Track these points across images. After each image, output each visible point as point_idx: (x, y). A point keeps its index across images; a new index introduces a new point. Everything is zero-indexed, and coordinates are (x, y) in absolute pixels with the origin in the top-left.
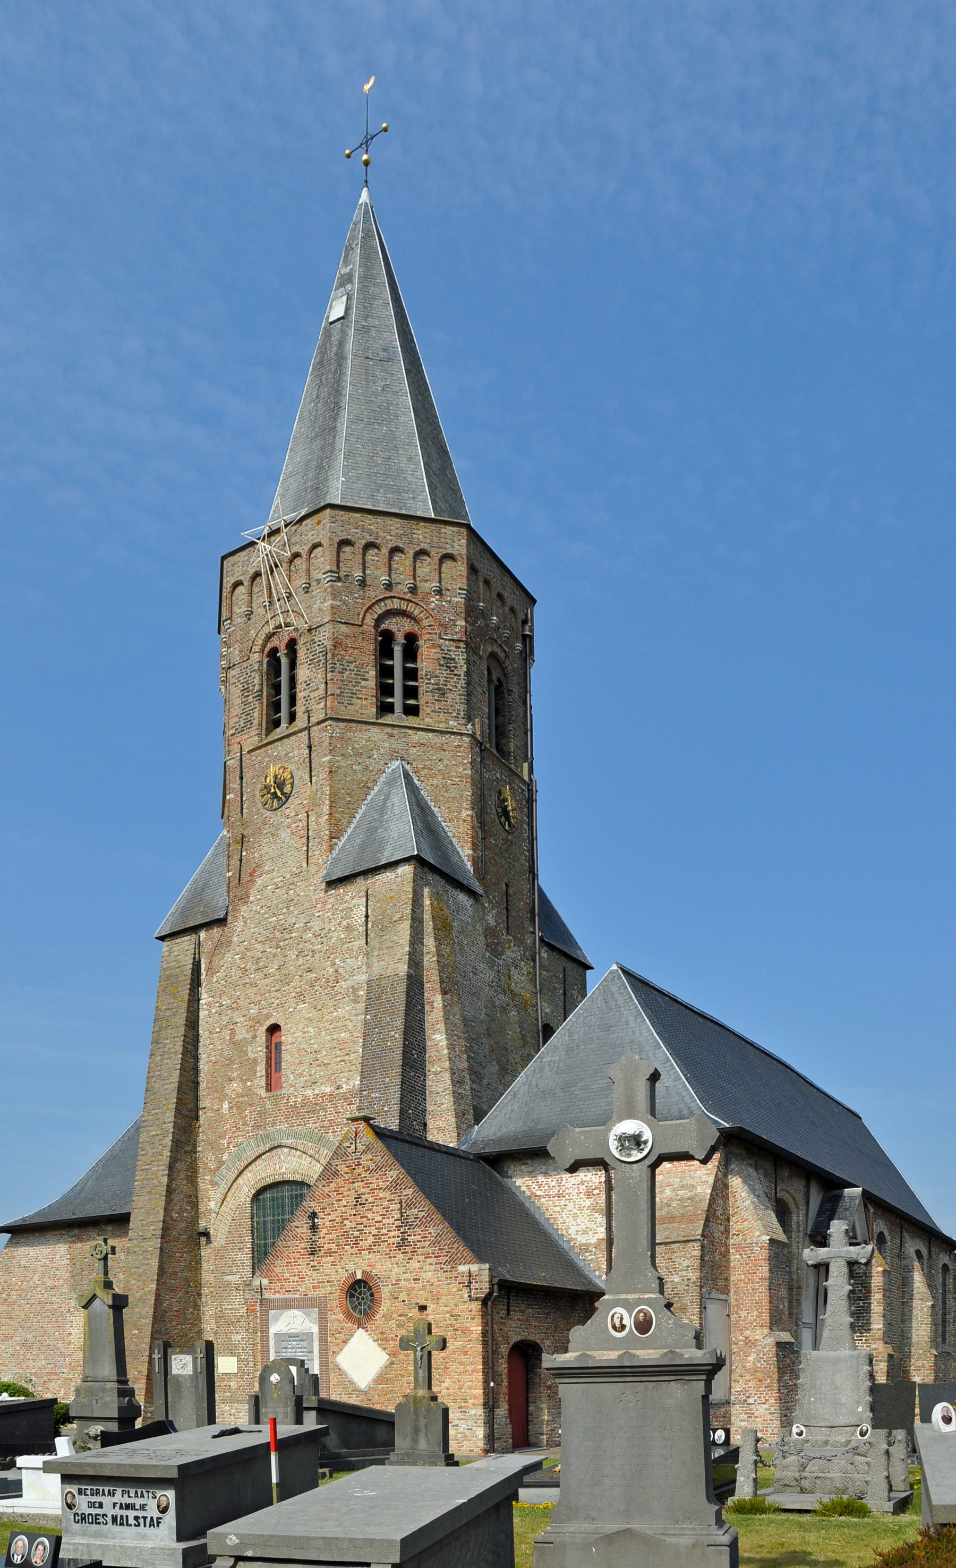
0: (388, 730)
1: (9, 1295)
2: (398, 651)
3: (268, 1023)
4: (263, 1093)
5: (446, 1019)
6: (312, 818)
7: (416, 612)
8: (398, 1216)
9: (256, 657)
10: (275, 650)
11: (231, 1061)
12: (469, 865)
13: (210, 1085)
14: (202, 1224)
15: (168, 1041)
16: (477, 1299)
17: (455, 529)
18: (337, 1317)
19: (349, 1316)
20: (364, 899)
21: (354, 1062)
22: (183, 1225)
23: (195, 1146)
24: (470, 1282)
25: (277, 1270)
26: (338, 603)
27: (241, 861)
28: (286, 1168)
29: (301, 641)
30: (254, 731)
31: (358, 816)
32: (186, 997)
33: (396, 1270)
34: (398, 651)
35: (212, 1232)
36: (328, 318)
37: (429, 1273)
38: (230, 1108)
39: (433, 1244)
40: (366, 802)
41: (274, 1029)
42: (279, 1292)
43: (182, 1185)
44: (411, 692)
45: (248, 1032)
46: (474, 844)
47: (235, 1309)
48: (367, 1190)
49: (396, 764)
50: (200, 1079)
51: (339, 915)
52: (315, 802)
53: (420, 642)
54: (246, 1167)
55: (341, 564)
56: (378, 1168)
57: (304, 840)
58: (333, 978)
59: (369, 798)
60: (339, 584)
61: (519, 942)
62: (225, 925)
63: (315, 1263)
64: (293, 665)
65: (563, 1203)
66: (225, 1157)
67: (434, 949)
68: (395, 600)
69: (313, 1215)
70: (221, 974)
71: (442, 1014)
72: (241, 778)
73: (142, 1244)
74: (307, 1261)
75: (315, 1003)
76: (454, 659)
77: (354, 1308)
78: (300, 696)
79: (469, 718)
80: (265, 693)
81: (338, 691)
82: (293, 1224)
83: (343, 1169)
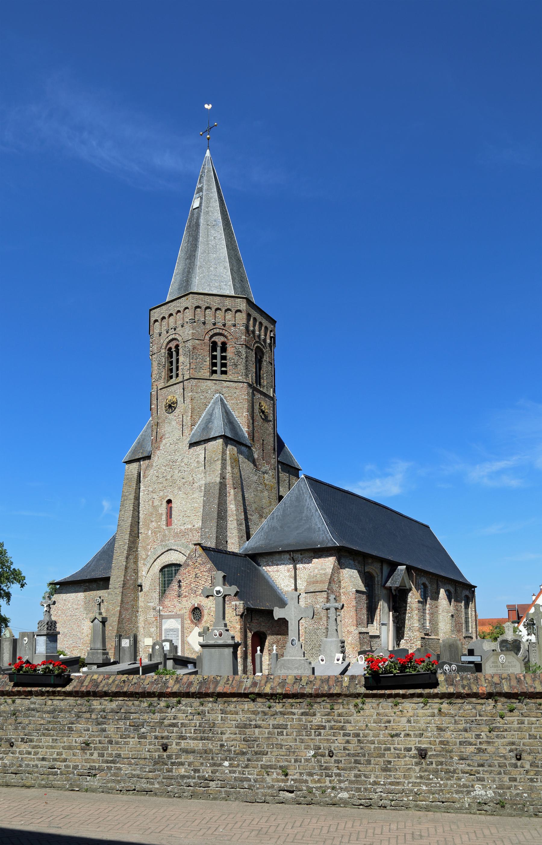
0: (214, 382)
2: (219, 349)
3: (167, 499)
4: (165, 527)
5: (235, 499)
6: (184, 417)
7: (226, 334)
8: (210, 582)
9: (163, 351)
10: (170, 349)
11: (152, 514)
12: (246, 435)
14: (140, 581)
17: (241, 299)
18: (188, 622)
19: (192, 621)
22: (132, 582)
23: (137, 548)
25: (166, 603)
26: (195, 331)
27: (157, 433)
29: (181, 346)
30: (162, 381)
31: (202, 417)
32: (135, 487)
34: (219, 349)
35: (143, 585)
36: (193, 206)
38: (152, 533)
40: (205, 411)
43: (132, 566)
44: (224, 365)
46: (248, 426)
48: (199, 572)
49: (217, 395)
50: (140, 521)
51: (194, 457)
52: (186, 412)
53: (228, 346)
54: (158, 558)
55: (196, 316)
56: (204, 563)
57: (181, 426)
58: (192, 482)
59: (207, 409)
60: (195, 324)
61: (268, 463)
62: (150, 459)
63: (180, 601)
64: (178, 354)
65: (278, 574)
66: (149, 553)
67: (230, 471)
68: (217, 329)
69: (180, 581)
70: (149, 478)
71: (233, 497)
72: (157, 399)
76: (241, 352)
77: (194, 618)
78: (180, 368)
79: (247, 375)
80: (166, 365)
81: (195, 367)
82: (172, 585)
83: (191, 563)
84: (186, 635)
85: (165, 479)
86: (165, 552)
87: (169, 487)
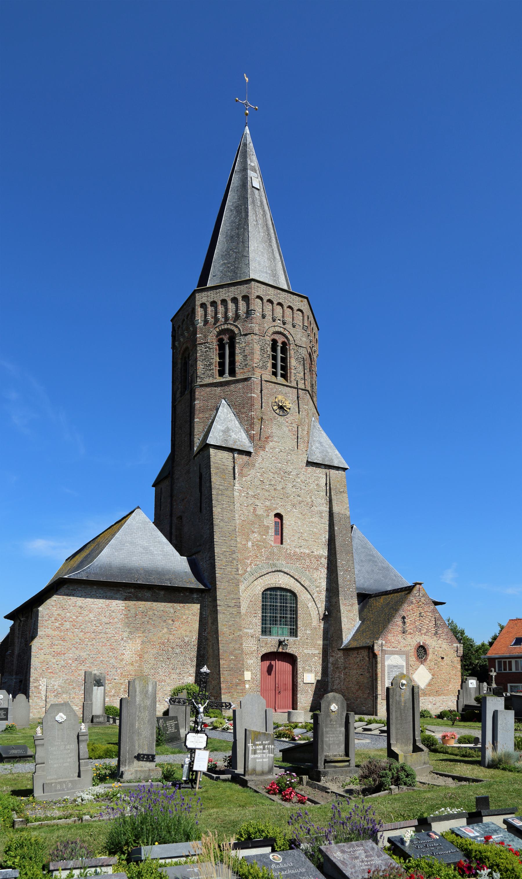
6: (300, 429)
8: (434, 623)
11: (253, 523)
13: (240, 531)
15: (225, 502)
16: (459, 656)
18: (413, 659)
20: (325, 476)
21: (320, 543)
24: (457, 650)
25: (389, 638)
28: (282, 582)
33: (434, 643)
37: (445, 646)
39: (446, 635)
41: (279, 516)
42: (389, 647)
45: (264, 512)
47: (250, 647)
48: (423, 611)
57: (296, 437)
58: (310, 504)
69: (404, 618)
70: (248, 478)
73: (228, 609)
74: (401, 636)
75: (301, 511)
82: (395, 620)
84: (411, 672)
85: (273, 488)
86: (270, 572)
87: (279, 499)
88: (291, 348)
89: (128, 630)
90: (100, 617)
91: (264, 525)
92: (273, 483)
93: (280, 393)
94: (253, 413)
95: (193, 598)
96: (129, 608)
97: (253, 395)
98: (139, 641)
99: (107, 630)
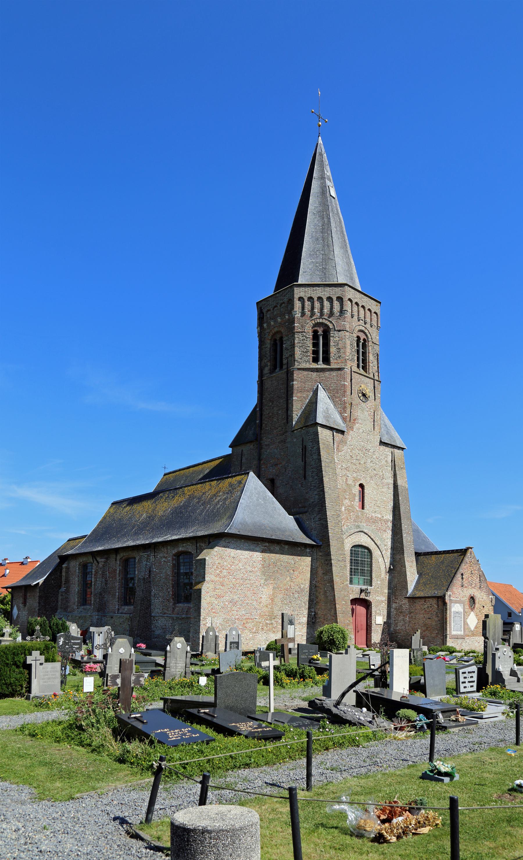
1: (221, 572)
6: (375, 414)
15: (330, 473)
18: (467, 607)
37: (485, 597)
58: (382, 477)
69: (462, 575)
70: (342, 453)
84: (466, 617)
88: (370, 344)
89: (264, 578)
90: (246, 566)
91: (352, 493)
92: (358, 458)
93: (363, 382)
94: (345, 398)
95: (307, 552)
96: (265, 559)
97: (346, 383)
98: (271, 587)
99: (251, 577)
